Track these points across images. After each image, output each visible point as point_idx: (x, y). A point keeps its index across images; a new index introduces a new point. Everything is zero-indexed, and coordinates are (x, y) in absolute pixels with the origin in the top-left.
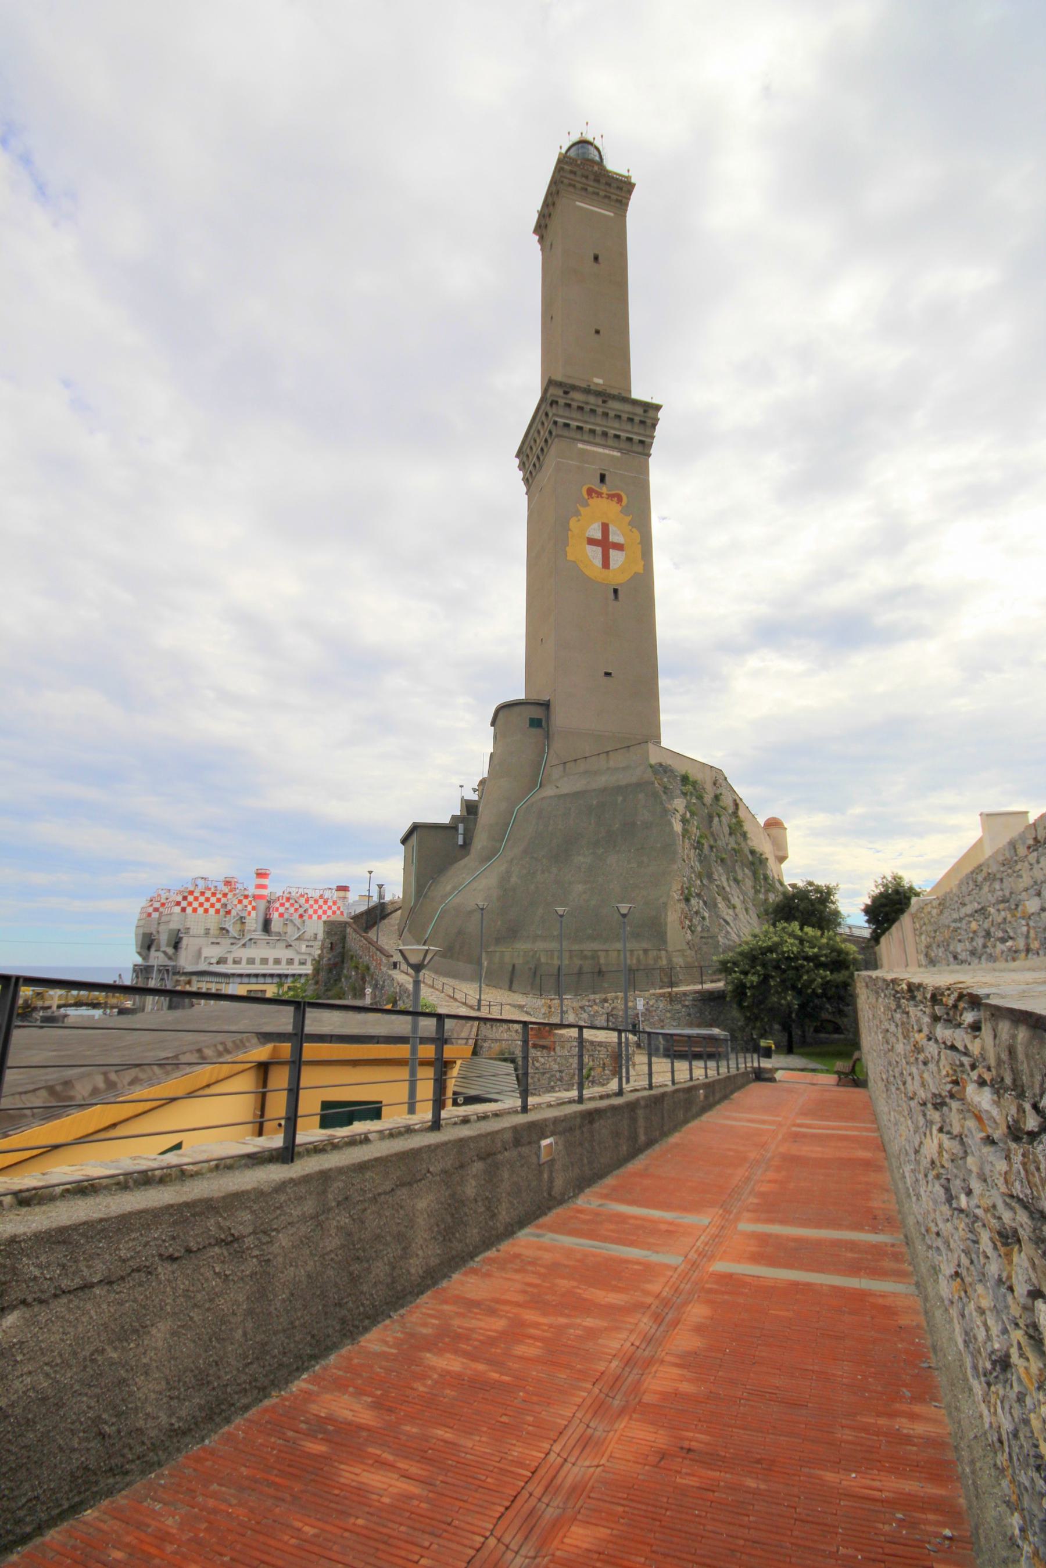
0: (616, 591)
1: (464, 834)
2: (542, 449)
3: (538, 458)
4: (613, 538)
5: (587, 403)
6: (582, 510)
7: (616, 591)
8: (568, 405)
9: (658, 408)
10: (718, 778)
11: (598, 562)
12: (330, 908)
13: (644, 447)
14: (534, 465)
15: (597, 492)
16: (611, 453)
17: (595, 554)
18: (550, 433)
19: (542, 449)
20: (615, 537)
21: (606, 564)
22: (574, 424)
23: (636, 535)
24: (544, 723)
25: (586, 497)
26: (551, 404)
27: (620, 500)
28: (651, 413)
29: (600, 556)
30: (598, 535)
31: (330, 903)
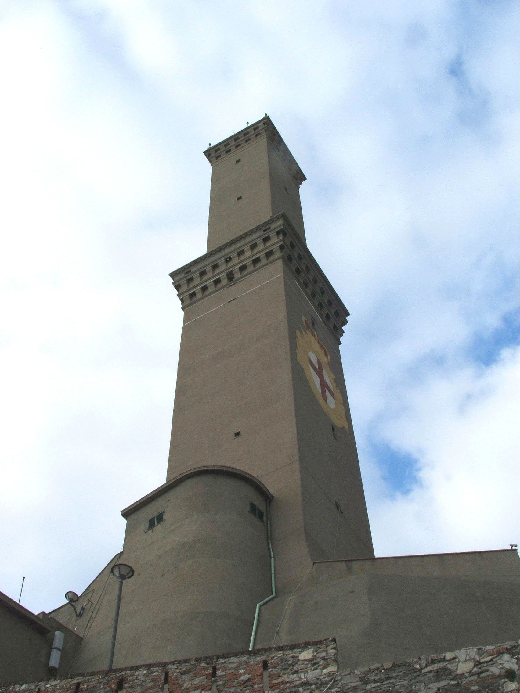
0: (333, 429)
3: (230, 277)
6: (304, 333)
7: (333, 429)
9: (348, 314)
24: (265, 518)
26: (278, 233)
27: (326, 355)
30: (316, 365)
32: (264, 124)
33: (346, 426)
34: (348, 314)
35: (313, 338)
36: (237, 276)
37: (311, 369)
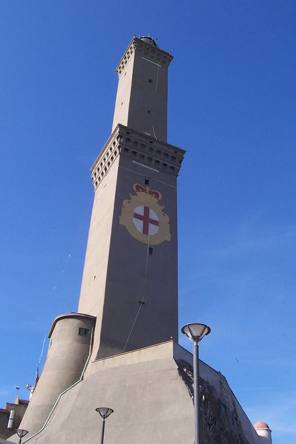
1: (14, 420)
2: (109, 164)
4: (153, 215)
5: (140, 141)
7: (151, 250)
8: (129, 140)
9: (184, 152)
10: (223, 380)
13: (174, 171)
14: (102, 173)
15: (142, 188)
16: (153, 170)
17: (139, 224)
18: (116, 153)
19: (109, 164)
21: (146, 230)
22: (131, 150)
23: (167, 219)
25: (136, 190)
26: (118, 138)
27: (157, 196)
28: (179, 153)
29: (142, 225)
30: (142, 213)
32: (133, 43)
33: (168, 238)
34: (184, 152)
35: (144, 193)
36: (108, 169)
37: (135, 220)
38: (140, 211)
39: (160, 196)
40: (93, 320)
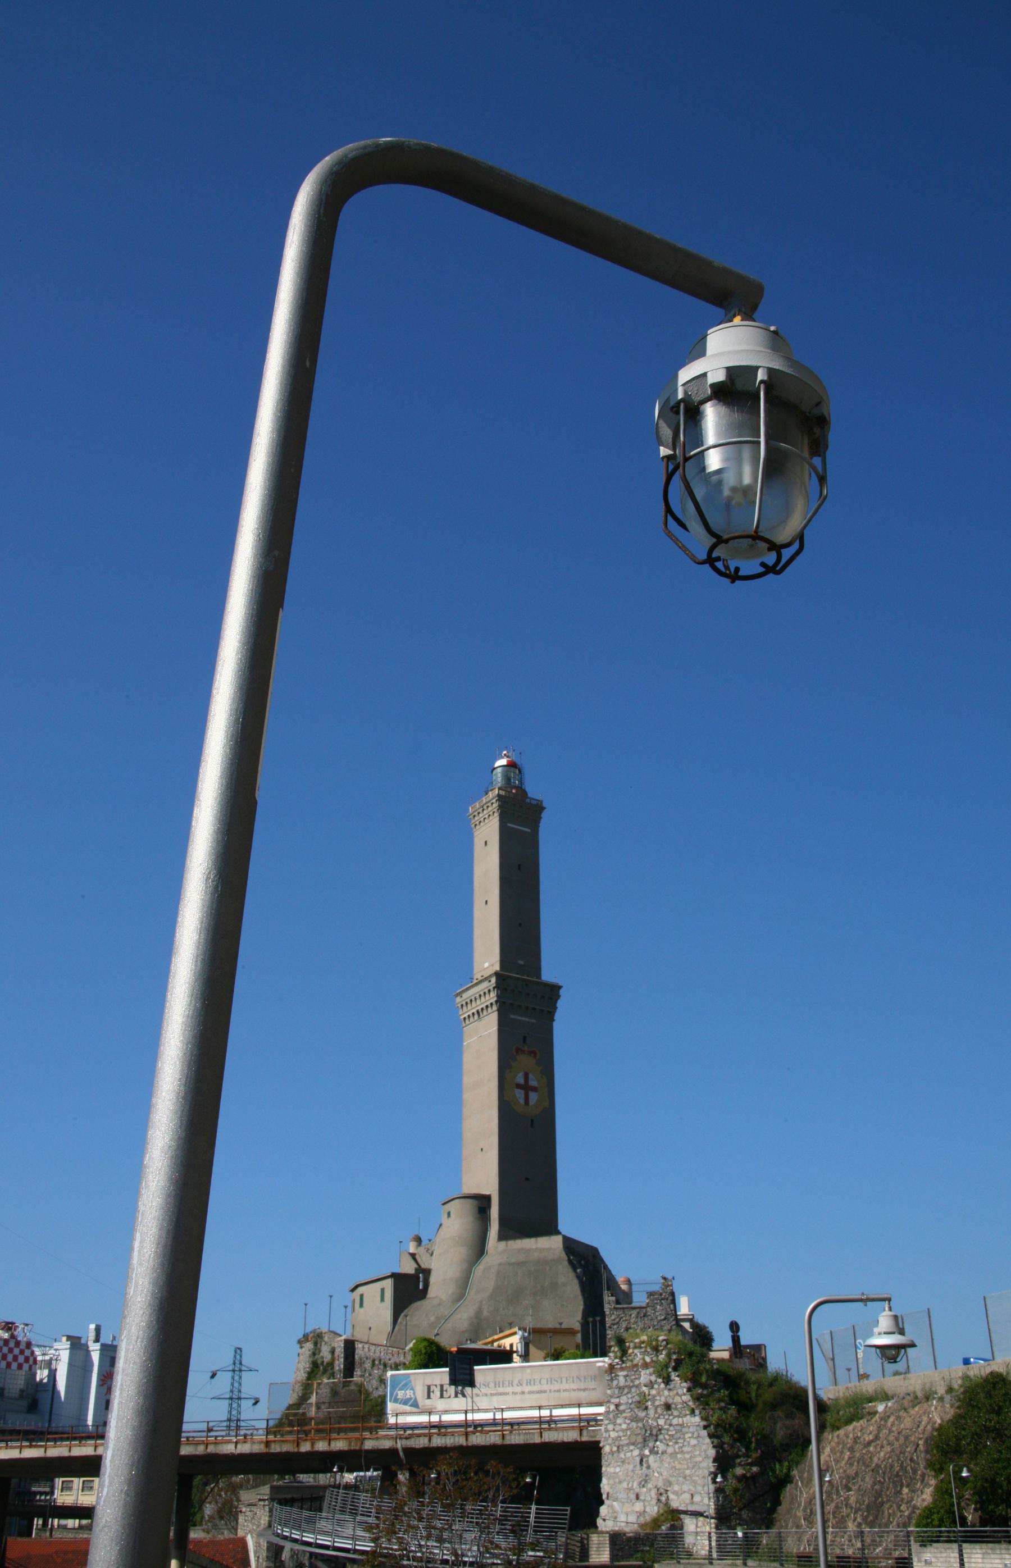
7: (532, 1121)
9: (560, 987)
11: (522, 1101)
12: (22, 1352)
17: (520, 1094)
20: (533, 1083)
31: (23, 1346)
34: (560, 987)
38: (520, 1079)
39: (538, 1055)
40: (487, 1199)
